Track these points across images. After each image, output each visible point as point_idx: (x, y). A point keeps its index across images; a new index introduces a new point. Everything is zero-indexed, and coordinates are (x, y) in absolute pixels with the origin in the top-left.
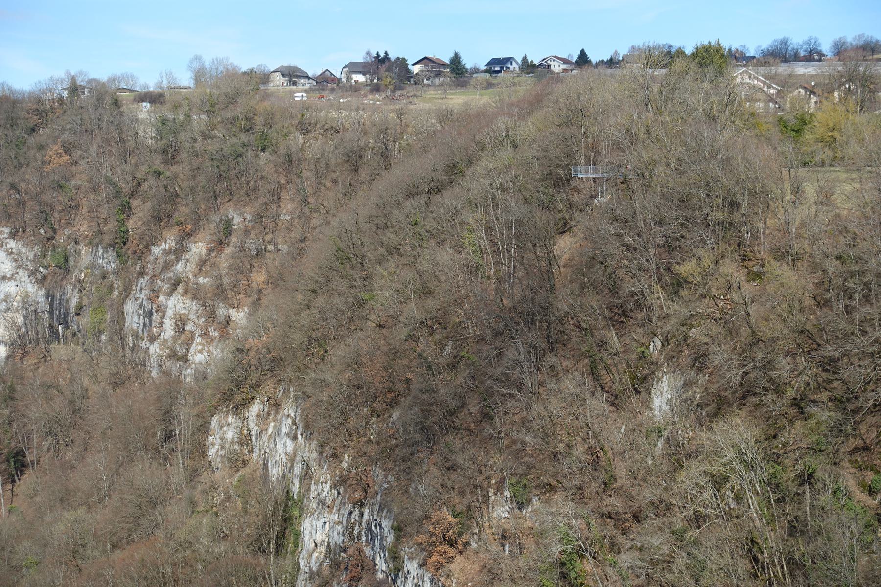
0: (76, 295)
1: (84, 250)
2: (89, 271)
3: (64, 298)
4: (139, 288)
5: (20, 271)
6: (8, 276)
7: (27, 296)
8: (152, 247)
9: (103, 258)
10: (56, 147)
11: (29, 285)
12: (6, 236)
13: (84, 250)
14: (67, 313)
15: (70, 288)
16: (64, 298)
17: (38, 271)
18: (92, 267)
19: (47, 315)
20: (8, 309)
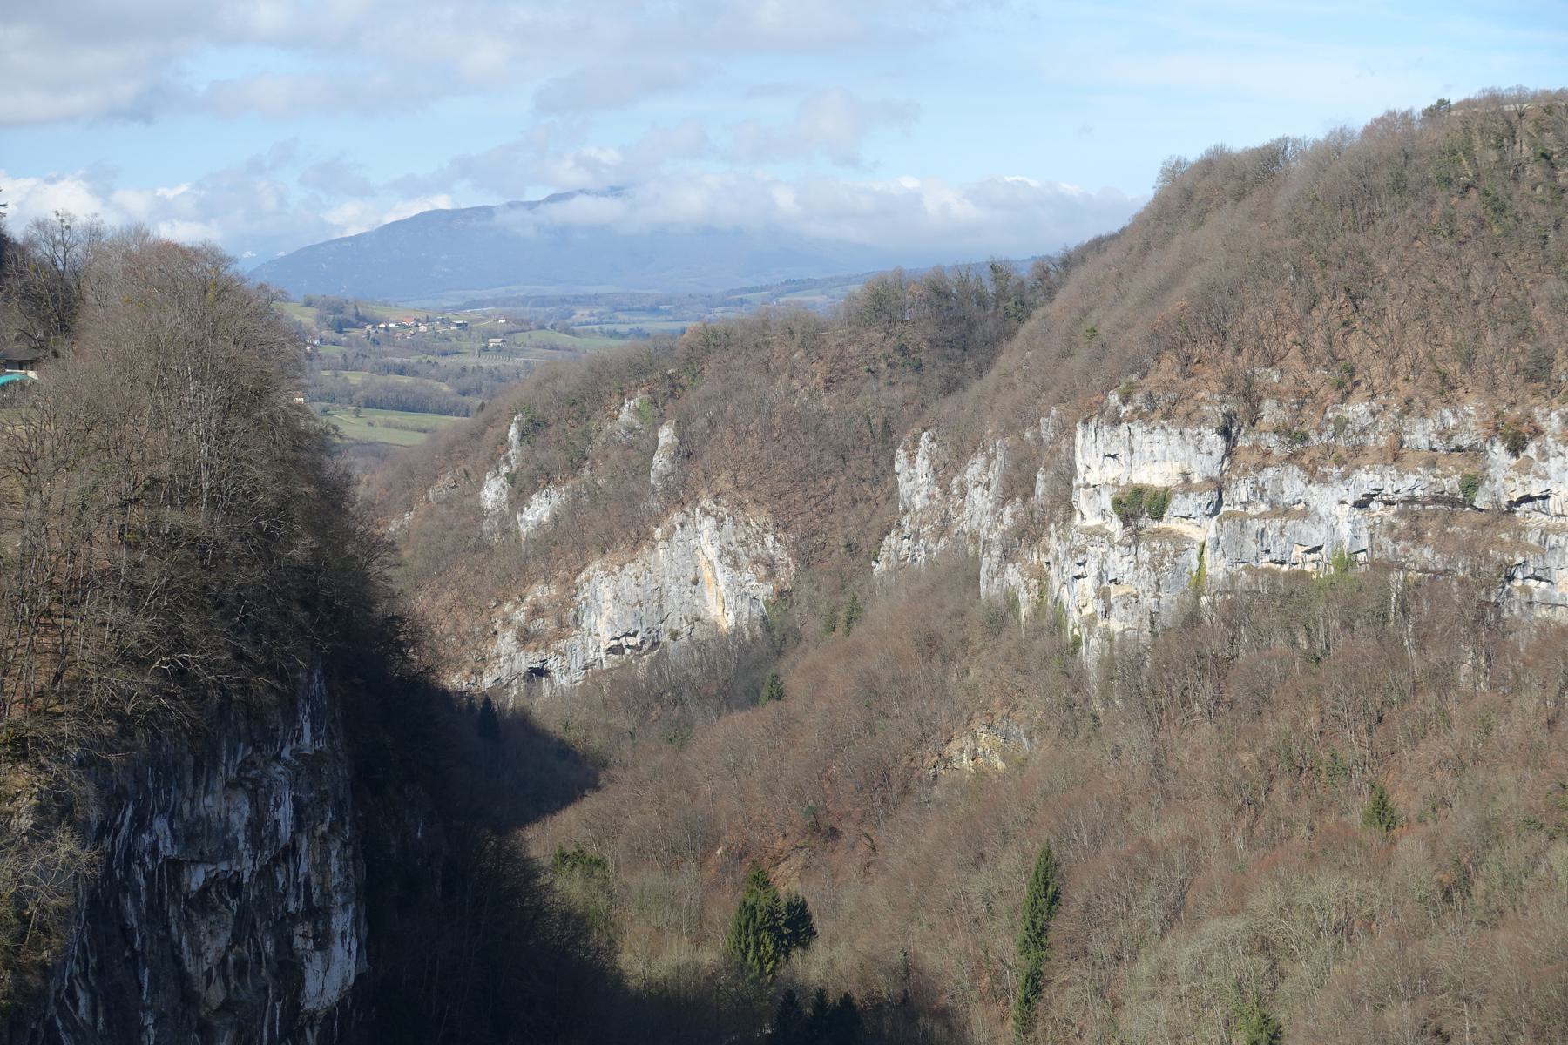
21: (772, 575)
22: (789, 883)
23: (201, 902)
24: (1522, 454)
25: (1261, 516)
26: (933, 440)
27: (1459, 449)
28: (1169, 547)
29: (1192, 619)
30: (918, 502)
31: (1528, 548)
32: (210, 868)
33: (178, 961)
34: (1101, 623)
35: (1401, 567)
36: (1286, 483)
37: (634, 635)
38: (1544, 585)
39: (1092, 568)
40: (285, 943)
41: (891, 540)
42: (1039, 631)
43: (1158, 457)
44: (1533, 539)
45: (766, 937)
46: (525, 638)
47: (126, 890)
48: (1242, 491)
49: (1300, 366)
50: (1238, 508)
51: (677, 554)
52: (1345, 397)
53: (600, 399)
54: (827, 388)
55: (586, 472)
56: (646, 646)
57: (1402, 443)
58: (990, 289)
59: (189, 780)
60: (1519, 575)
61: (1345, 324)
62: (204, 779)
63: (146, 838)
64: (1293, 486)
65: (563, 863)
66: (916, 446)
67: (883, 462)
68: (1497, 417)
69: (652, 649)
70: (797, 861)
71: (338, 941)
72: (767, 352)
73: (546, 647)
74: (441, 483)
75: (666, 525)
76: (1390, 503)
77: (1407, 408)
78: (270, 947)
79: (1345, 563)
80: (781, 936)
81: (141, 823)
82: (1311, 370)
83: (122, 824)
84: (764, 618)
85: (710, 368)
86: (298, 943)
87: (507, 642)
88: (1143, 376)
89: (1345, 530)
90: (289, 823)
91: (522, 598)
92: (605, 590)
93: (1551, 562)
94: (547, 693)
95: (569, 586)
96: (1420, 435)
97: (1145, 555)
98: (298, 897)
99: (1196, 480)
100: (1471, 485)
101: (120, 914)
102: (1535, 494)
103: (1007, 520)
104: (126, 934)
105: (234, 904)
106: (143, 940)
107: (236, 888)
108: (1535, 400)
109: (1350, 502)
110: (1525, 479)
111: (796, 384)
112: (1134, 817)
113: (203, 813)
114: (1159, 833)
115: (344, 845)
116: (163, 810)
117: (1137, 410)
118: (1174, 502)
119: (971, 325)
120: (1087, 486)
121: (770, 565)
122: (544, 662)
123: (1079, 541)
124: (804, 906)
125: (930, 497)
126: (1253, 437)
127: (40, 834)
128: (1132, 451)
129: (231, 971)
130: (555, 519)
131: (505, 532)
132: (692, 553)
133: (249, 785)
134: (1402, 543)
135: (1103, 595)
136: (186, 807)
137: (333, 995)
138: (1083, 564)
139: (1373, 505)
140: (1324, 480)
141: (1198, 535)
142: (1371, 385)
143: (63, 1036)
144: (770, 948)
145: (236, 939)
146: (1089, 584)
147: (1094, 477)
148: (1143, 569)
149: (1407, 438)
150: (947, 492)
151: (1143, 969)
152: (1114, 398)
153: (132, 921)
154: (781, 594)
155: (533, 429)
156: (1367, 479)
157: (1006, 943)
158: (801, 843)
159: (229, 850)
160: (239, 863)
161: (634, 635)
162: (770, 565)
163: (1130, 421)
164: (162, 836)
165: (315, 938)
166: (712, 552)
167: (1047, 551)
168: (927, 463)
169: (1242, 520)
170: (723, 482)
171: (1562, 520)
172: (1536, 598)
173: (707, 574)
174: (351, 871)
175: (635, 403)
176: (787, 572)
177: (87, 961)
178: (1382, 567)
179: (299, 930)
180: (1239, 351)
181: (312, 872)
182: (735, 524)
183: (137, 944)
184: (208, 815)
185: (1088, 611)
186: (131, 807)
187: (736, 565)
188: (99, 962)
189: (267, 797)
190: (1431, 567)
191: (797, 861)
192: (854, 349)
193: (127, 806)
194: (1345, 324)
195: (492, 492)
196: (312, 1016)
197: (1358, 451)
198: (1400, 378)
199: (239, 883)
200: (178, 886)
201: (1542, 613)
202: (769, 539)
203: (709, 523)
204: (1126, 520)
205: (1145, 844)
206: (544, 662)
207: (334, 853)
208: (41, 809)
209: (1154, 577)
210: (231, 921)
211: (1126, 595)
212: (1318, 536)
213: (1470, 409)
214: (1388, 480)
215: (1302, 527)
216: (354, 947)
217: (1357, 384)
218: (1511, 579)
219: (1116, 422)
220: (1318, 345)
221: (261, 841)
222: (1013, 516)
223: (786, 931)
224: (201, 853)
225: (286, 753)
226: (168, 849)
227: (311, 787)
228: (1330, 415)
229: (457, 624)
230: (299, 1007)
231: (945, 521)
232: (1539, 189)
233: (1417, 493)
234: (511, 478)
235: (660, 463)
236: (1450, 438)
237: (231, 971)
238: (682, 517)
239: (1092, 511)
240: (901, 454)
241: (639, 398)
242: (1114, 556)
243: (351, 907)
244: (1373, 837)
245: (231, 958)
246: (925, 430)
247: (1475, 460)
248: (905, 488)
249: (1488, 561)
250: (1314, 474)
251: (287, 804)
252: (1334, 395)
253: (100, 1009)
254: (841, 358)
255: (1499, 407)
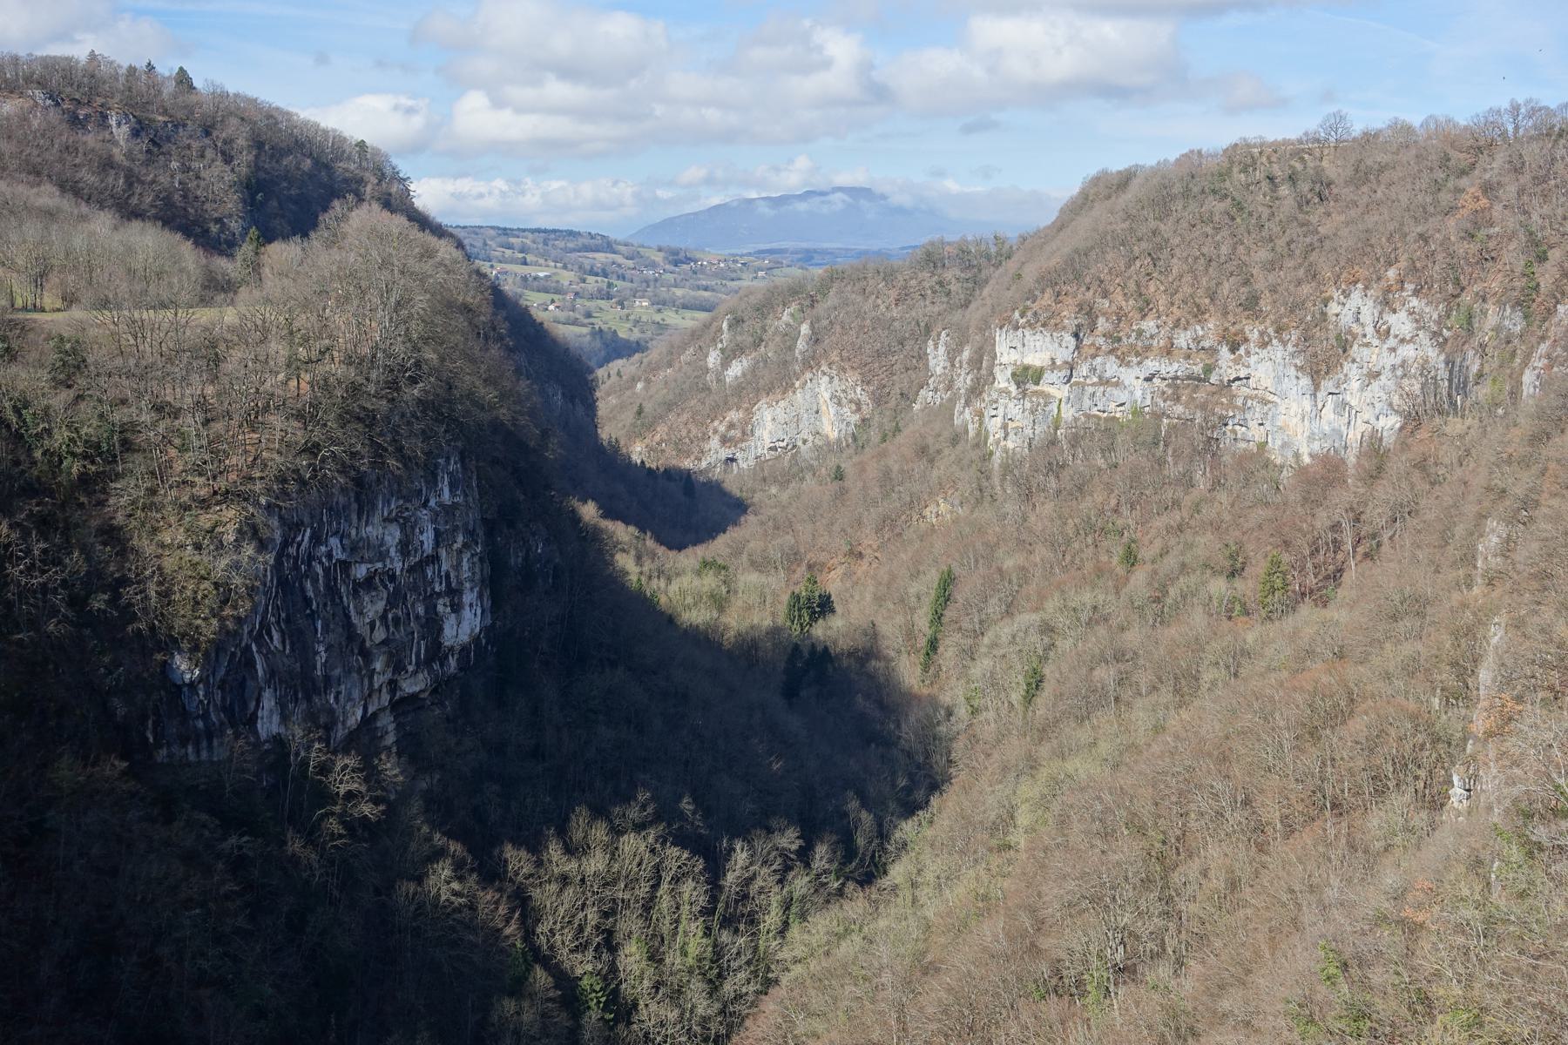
0: (1478, 362)
1: (1492, 309)
2: (1494, 333)
3: (1465, 364)
4: (1538, 355)
5: (1421, 333)
6: (1408, 338)
7: (1426, 361)
8: (1559, 306)
9: (1511, 319)
10: (1472, 190)
11: (1430, 349)
12: (1410, 293)
13: (1492, 309)
14: (1465, 384)
15: (1471, 353)
16: (1465, 364)
17: (1441, 335)
18: (1497, 329)
19: (1446, 383)
20: (1405, 375)
21: (859, 409)
22: (833, 584)
23: (369, 583)
24: (1237, 353)
25: (1093, 385)
26: (948, 335)
27: (1203, 349)
28: (1041, 401)
29: (1053, 442)
30: (939, 370)
31: (1236, 407)
32: (369, 566)
33: (348, 617)
34: (1002, 443)
35: (1168, 417)
36: (1108, 366)
37: (783, 441)
38: (1244, 428)
39: (1001, 411)
40: (431, 609)
41: (922, 392)
42: (977, 445)
43: (1038, 349)
44: (1239, 402)
45: (805, 613)
46: (725, 441)
47: (307, 577)
48: (1084, 369)
49: (1120, 298)
50: (1082, 380)
51: (807, 397)
52: (1144, 317)
53: (773, 308)
54: (896, 304)
55: (763, 349)
56: (789, 447)
57: (1173, 344)
58: (993, 250)
59: (354, 517)
60: (1230, 423)
61: (1148, 274)
62: (365, 517)
63: (323, 549)
64: (1111, 367)
65: (705, 566)
66: (939, 339)
67: (923, 346)
68: (1224, 331)
69: (792, 449)
70: (840, 570)
71: (467, 608)
72: (865, 283)
73: (735, 446)
74: (687, 352)
75: (802, 379)
76: (1165, 379)
77: (1177, 325)
78: (421, 610)
79: (1137, 412)
80: (815, 612)
81: (317, 539)
82: (1127, 301)
83: (303, 540)
84: (853, 434)
85: (832, 292)
86: (440, 608)
87: (714, 442)
88: (1034, 302)
89: (1138, 394)
90: (431, 542)
91: (724, 418)
92: (768, 415)
93: (1248, 416)
94: (735, 472)
95: (749, 411)
96: (1183, 339)
97: (1028, 405)
98: (441, 583)
99: (1058, 362)
100: (1208, 370)
101: (303, 590)
102: (1242, 376)
103: (968, 382)
104: (307, 602)
105: (391, 587)
106: (318, 605)
107: (393, 578)
108: (1248, 321)
109: (1142, 378)
110: (1237, 367)
111: (879, 301)
112: (1000, 553)
113: (364, 535)
114: (1009, 564)
115: (472, 555)
116: (335, 534)
117: (1029, 321)
118: (1046, 375)
119: (980, 271)
120: (1001, 364)
121: (858, 404)
122: (734, 454)
123: (995, 396)
124: (830, 596)
125: (945, 368)
126: (1091, 339)
127: (237, 545)
128: (1024, 345)
129: (390, 623)
130: (744, 374)
131: (719, 381)
132: (816, 396)
133: (401, 521)
134: (1168, 402)
135: (1005, 427)
136: (353, 532)
137: (464, 638)
138: (996, 409)
139: (1155, 380)
140: (1128, 365)
141: (1058, 394)
142: (1158, 311)
143: (256, 655)
144: (807, 619)
145: (392, 602)
146: (999, 421)
147: (1004, 360)
148: (1027, 413)
149: (1175, 341)
150: (953, 365)
151: (986, 640)
152: (1017, 314)
153: (311, 594)
154: (863, 420)
155: (737, 322)
156: (1151, 365)
157: (922, 621)
158: (843, 561)
159: (383, 556)
160: (392, 563)
161: (783, 441)
162: (858, 404)
163: (1024, 328)
164: (335, 547)
165: (452, 606)
166: (827, 396)
167: (984, 400)
168: (944, 348)
169: (1082, 386)
170: (834, 356)
171: (1256, 392)
172: (1239, 436)
173: (824, 408)
174: (477, 570)
175: (791, 310)
176: (866, 410)
177: (280, 615)
178: (1158, 416)
179: (441, 601)
180: (1088, 289)
181: (451, 570)
182: (840, 380)
183: (314, 607)
184: (368, 537)
185: (997, 436)
186: (309, 530)
187: (839, 404)
188: (288, 616)
189: (413, 528)
190: (1183, 416)
191: (840, 570)
192: (913, 282)
193: (305, 531)
194: (1148, 274)
195: (713, 359)
196: (451, 649)
197: (1148, 348)
198: (1176, 306)
199: (394, 574)
200: (348, 576)
201: (1243, 445)
202: (859, 389)
203: (826, 379)
204: (1018, 385)
205: (1000, 570)
206: (734, 454)
207: (465, 560)
208: (239, 531)
209: (1032, 418)
210: (385, 596)
211: (1017, 428)
212: (1123, 396)
213: (1211, 326)
214: (1163, 365)
215: (1116, 392)
216: (479, 612)
217: (1151, 309)
218: (1226, 425)
219: (1016, 328)
220: (1132, 286)
221: (409, 552)
222: (972, 380)
223: (817, 609)
224: (362, 557)
225: (432, 503)
226: (339, 554)
227: (446, 522)
228: (1134, 327)
229: (689, 432)
230: (440, 644)
231: (952, 381)
232: (1268, 198)
233: (1179, 373)
234: (723, 351)
235: (801, 345)
236: (1199, 342)
237: (390, 623)
238: (810, 375)
239: (1003, 380)
240: (930, 343)
241: (794, 307)
242: (1011, 405)
243: (477, 589)
244: (1120, 570)
245: (390, 616)
246: (944, 329)
247: (1212, 356)
248: (932, 363)
249: (1214, 414)
250: (1123, 362)
251: (430, 532)
252: (1138, 316)
253: (287, 642)
254: (905, 288)
255: (1227, 325)
